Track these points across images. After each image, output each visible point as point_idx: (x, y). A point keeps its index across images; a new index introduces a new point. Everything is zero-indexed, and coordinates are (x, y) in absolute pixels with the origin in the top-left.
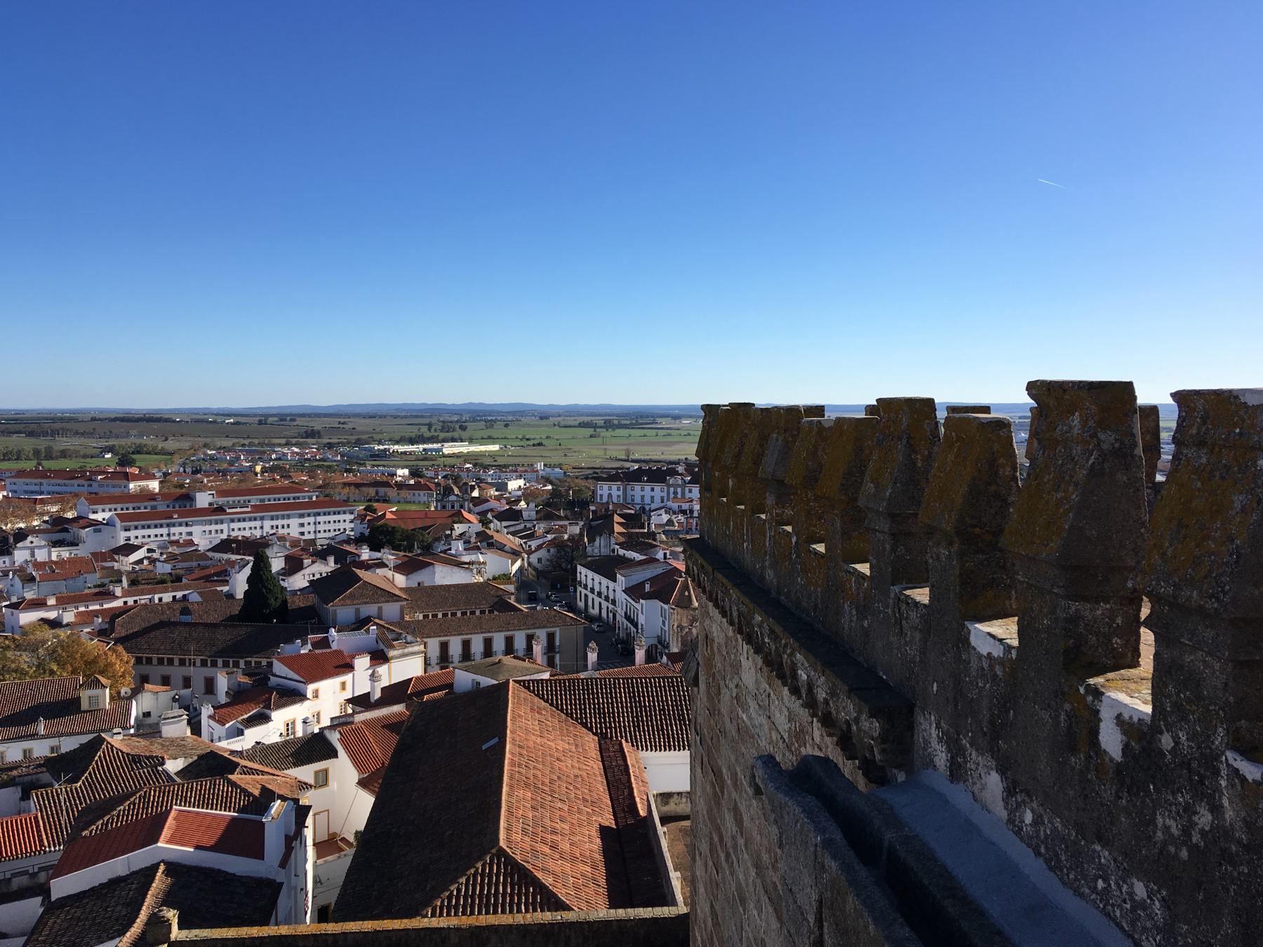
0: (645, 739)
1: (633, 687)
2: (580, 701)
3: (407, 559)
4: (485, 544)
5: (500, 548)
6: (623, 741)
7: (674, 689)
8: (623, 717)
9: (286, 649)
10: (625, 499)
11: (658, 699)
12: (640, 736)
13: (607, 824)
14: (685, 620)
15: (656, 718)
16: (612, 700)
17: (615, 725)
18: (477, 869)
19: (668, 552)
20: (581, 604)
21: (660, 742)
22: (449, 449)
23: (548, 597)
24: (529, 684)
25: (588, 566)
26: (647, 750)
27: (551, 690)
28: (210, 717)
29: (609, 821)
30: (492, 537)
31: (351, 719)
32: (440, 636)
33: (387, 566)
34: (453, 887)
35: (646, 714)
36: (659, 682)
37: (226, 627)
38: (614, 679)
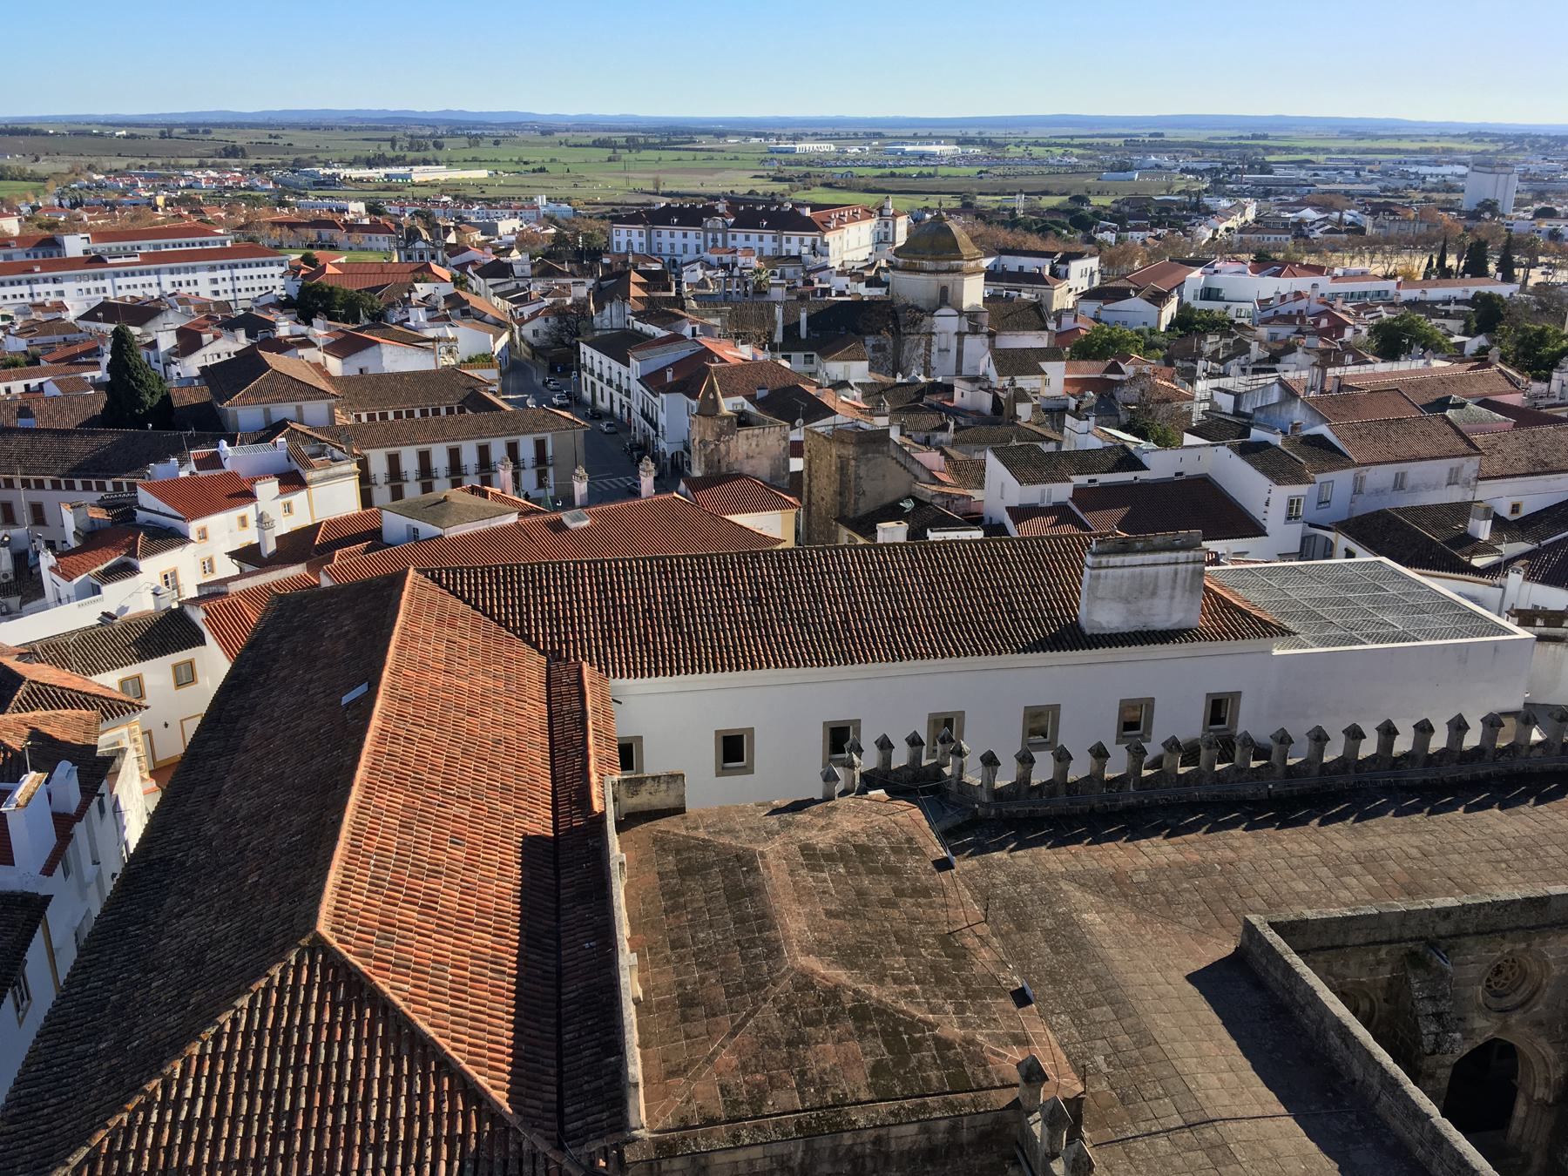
0: (620, 659)
1: (604, 576)
2: (520, 600)
3: (342, 335)
4: (457, 312)
5: (480, 317)
6: (585, 665)
8: (587, 624)
9: (157, 470)
10: (650, 248)
11: (641, 593)
12: (612, 654)
13: (540, 830)
14: (709, 432)
16: (571, 597)
17: (574, 637)
18: (272, 978)
19: (697, 326)
20: (587, 395)
21: (642, 664)
22: (420, 174)
23: (545, 384)
24: (440, 574)
25: (596, 345)
26: (622, 676)
27: (476, 584)
28: (52, 569)
30: (467, 302)
31: (223, 589)
32: (386, 446)
33: (315, 345)
34: (225, 1018)
35: (623, 617)
37: (81, 433)
38: (575, 563)
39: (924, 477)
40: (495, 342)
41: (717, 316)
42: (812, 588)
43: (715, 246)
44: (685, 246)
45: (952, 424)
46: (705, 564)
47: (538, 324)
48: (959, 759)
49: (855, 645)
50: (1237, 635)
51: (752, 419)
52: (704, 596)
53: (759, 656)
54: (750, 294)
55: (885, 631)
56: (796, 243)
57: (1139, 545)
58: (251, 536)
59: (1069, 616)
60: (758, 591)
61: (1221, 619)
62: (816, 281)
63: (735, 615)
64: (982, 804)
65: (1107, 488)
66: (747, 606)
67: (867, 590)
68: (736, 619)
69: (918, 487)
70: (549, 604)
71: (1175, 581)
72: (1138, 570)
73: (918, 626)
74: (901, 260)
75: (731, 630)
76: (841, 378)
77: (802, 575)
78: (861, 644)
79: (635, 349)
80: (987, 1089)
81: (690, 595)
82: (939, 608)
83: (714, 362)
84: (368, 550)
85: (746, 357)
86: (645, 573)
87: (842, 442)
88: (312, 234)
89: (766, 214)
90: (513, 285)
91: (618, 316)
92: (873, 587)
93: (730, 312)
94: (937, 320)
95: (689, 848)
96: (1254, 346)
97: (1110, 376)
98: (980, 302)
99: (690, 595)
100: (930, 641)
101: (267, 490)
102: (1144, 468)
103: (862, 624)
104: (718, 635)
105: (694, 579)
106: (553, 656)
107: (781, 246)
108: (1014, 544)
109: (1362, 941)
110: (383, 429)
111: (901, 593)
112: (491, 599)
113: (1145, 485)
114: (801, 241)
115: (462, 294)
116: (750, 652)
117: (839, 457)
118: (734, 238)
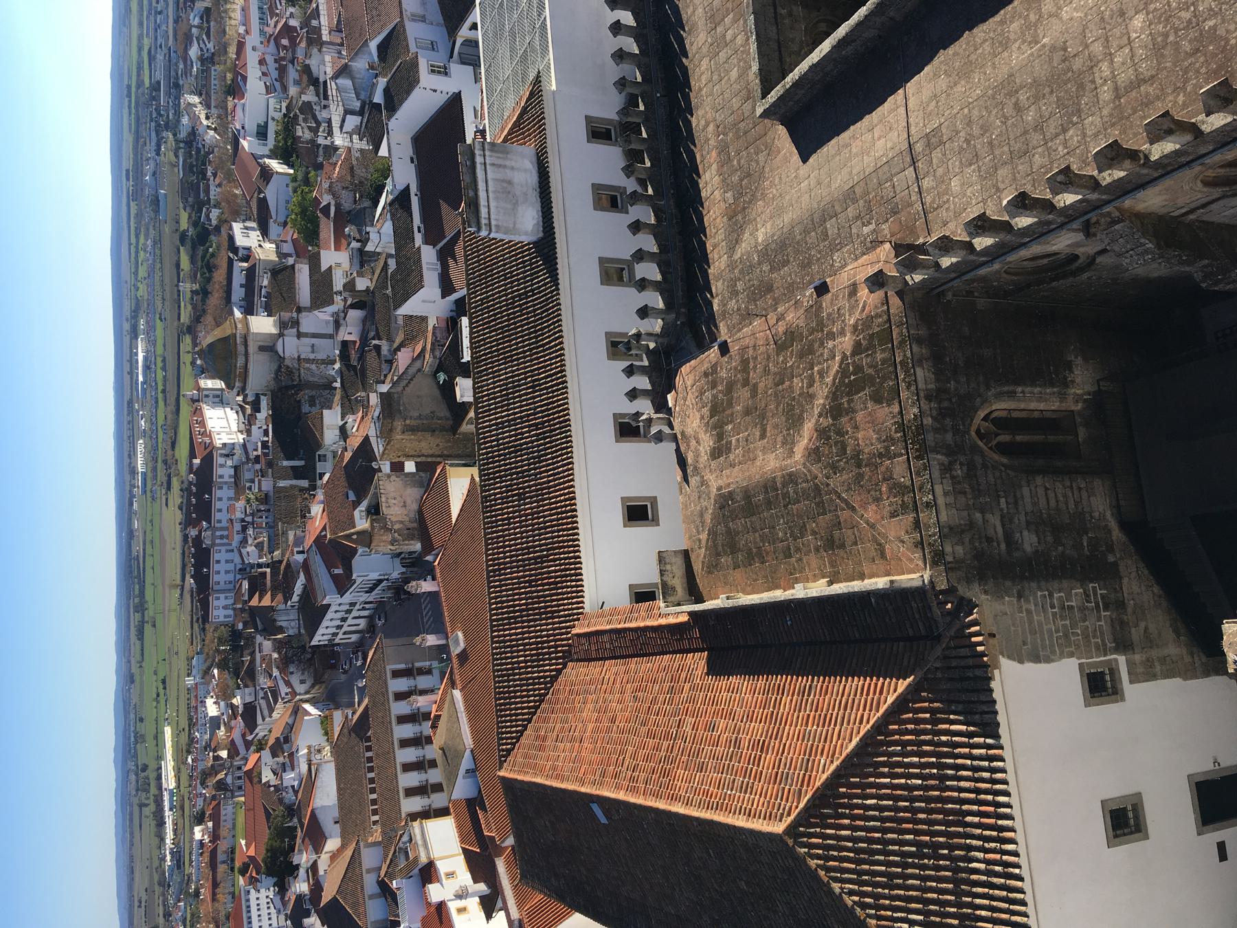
0: (569, 604)
2: (524, 685)
3: (307, 839)
4: (286, 747)
5: (290, 728)
6: (575, 631)
7: (503, 569)
10: (229, 590)
11: (516, 589)
12: (565, 610)
14: (384, 538)
15: (540, 591)
16: (520, 645)
17: (552, 641)
18: (818, 866)
19: (296, 549)
20: (354, 637)
21: (572, 587)
22: (170, 782)
23: (345, 672)
24: (503, 750)
26: (583, 602)
27: (511, 721)
29: (697, 662)
30: (277, 739)
31: (516, 923)
32: (399, 799)
33: (316, 861)
34: (849, 901)
35: (536, 603)
36: (495, 587)
38: (493, 642)
39: (418, 364)
40: (310, 715)
41: (287, 534)
42: (510, 453)
43: (227, 537)
44: (227, 561)
45: (374, 342)
46: (492, 539)
47: (295, 680)
48: (643, 336)
49: (555, 419)
50: (541, 118)
51: (374, 503)
52: (518, 538)
53: (564, 494)
54: (267, 507)
55: (544, 394)
56: (223, 470)
57: (471, 194)
58: (473, 904)
59: (529, 249)
60: (513, 496)
61: (529, 130)
62: (255, 453)
63: (532, 514)
64: (677, 318)
65: (424, 219)
67: (511, 409)
69: (426, 369)
70: (526, 662)
71: (499, 166)
72: (491, 195)
74: (237, 384)
75: (544, 517)
76: (337, 432)
77: (499, 461)
78: (554, 413)
79: (315, 598)
80: (889, 316)
81: (517, 550)
82: (524, 352)
83: (326, 536)
84: (484, 808)
85: (321, 509)
86: (500, 586)
87: (391, 430)
88: (222, 868)
89: (199, 495)
90: (263, 702)
91: (288, 614)
92: (508, 405)
94: (287, 355)
95: (715, 546)
96: (305, 98)
97: (332, 215)
98: (271, 319)
99: (517, 550)
100: (551, 359)
101: (436, 893)
102: (408, 188)
103: (538, 413)
104: (549, 527)
105: (504, 547)
106: (566, 657)
107: (226, 483)
108: (472, 293)
109: (774, 28)
110: (385, 803)
111: (513, 382)
112: (523, 708)
113: (421, 187)
114: (222, 466)
115: (271, 742)
116: (562, 501)
118: (219, 521)
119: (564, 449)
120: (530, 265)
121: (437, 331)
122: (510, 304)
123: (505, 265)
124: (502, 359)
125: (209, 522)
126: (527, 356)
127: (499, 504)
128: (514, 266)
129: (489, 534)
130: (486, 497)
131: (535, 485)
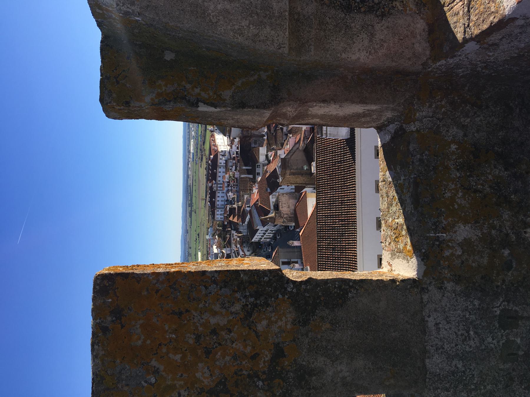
10: (222, 208)
20: (268, 240)
39: (297, 146)
41: (244, 196)
42: (330, 229)
43: (222, 187)
44: (222, 197)
46: (321, 264)
51: (277, 203)
52: (331, 266)
54: (237, 184)
55: (346, 207)
56: (221, 161)
59: (344, 142)
66: (335, 253)
67: (332, 210)
68: (339, 257)
69: (301, 148)
73: (344, 196)
74: (227, 134)
75: (343, 260)
76: (265, 157)
77: (326, 232)
82: (339, 187)
83: (258, 204)
85: (257, 191)
87: (285, 174)
89: (212, 170)
92: (331, 208)
93: (242, 192)
103: (343, 215)
104: (345, 265)
107: (222, 166)
108: (318, 157)
111: (333, 199)
114: (221, 159)
116: (351, 256)
117: (290, 175)
118: (219, 181)
119: (353, 233)
120: (344, 149)
121: (306, 132)
122: (334, 164)
123: (332, 147)
124: (329, 188)
125: (216, 181)
126: (340, 189)
127: (324, 250)
128: (336, 148)
129: (320, 261)
130: (319, 245)
131: (340, 246)
